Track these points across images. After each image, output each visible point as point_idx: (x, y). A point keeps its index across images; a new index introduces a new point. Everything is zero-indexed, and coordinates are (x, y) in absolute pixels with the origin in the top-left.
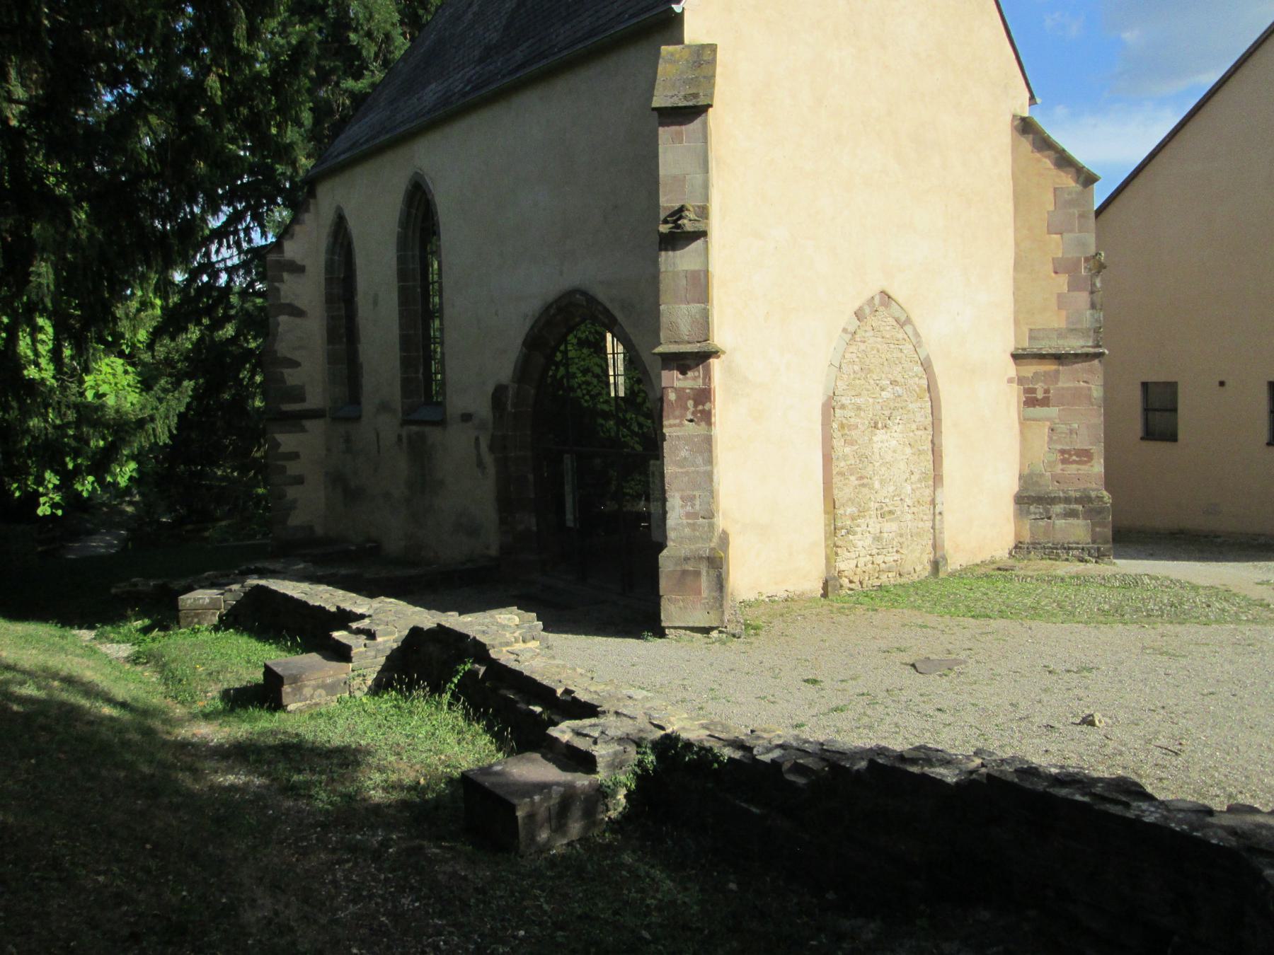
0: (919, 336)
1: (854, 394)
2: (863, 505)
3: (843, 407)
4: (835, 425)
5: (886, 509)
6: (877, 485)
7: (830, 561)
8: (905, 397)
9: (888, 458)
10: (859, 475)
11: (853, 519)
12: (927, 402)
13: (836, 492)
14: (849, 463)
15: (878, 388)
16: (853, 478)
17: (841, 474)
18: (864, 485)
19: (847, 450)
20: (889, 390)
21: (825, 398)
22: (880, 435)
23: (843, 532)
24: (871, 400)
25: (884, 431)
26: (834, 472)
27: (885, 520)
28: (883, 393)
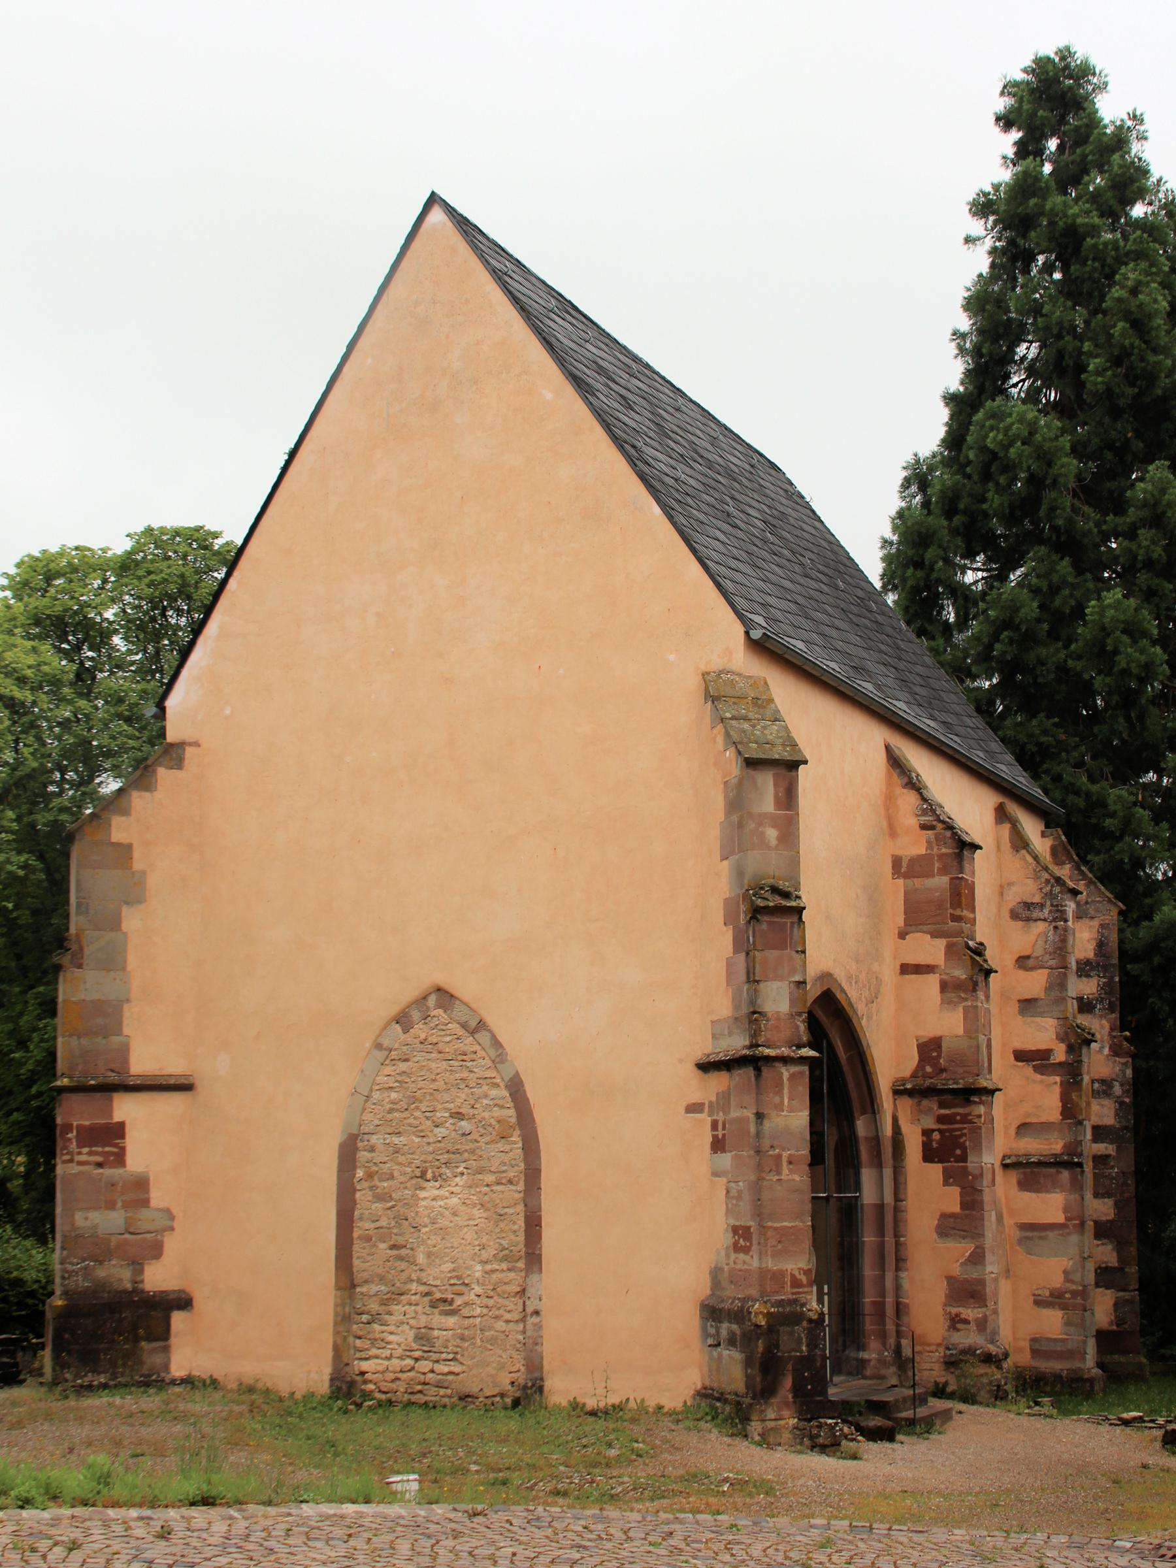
0: (501, 1046)
1: (389, 1130)
2: (398, 1284)
3: (372, 1149)
4: (360, 1173)
5: (438, 1295)
6: (421, 1259)
7: (337, 1351)
8: (475, 1136)
9: (443, 1223)
10: (392, 1243)
11: (384, 1303)
12: (514, 1143)
13: (356, 1262)
14: (378, 1224)
15: (429, 1123)
16: (383, 1246)
17: (368, 1239)
18: (401, 1258)
19: (378, 1206)
20: (447, 1125)
21: (345, 1137)
22: (431, 1190)
23: (365, 1318)
24: (417, 1140)
25: (437, 1184)
26: (355, 1235)
27: (436, 1311)
28: (437, 1130)
